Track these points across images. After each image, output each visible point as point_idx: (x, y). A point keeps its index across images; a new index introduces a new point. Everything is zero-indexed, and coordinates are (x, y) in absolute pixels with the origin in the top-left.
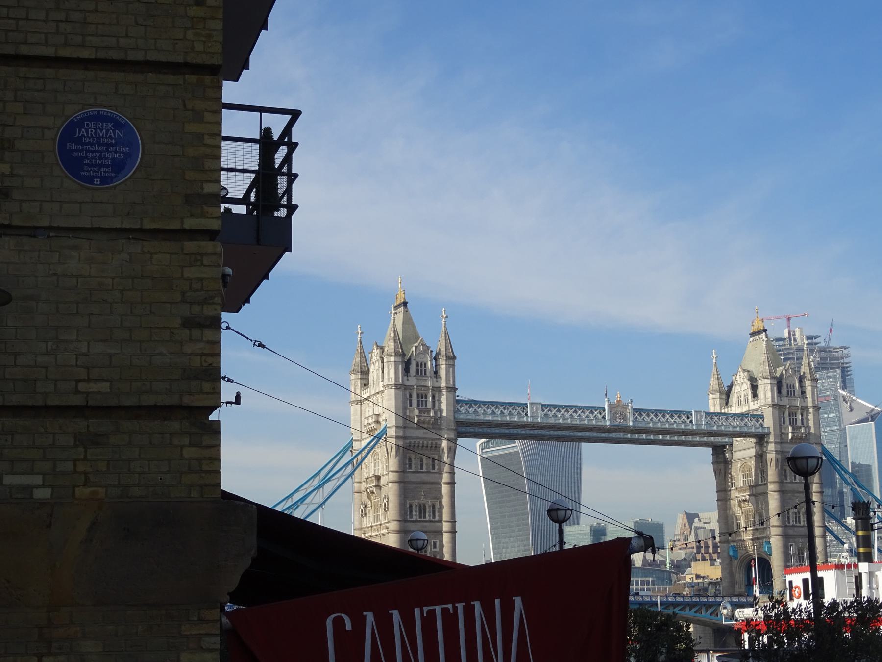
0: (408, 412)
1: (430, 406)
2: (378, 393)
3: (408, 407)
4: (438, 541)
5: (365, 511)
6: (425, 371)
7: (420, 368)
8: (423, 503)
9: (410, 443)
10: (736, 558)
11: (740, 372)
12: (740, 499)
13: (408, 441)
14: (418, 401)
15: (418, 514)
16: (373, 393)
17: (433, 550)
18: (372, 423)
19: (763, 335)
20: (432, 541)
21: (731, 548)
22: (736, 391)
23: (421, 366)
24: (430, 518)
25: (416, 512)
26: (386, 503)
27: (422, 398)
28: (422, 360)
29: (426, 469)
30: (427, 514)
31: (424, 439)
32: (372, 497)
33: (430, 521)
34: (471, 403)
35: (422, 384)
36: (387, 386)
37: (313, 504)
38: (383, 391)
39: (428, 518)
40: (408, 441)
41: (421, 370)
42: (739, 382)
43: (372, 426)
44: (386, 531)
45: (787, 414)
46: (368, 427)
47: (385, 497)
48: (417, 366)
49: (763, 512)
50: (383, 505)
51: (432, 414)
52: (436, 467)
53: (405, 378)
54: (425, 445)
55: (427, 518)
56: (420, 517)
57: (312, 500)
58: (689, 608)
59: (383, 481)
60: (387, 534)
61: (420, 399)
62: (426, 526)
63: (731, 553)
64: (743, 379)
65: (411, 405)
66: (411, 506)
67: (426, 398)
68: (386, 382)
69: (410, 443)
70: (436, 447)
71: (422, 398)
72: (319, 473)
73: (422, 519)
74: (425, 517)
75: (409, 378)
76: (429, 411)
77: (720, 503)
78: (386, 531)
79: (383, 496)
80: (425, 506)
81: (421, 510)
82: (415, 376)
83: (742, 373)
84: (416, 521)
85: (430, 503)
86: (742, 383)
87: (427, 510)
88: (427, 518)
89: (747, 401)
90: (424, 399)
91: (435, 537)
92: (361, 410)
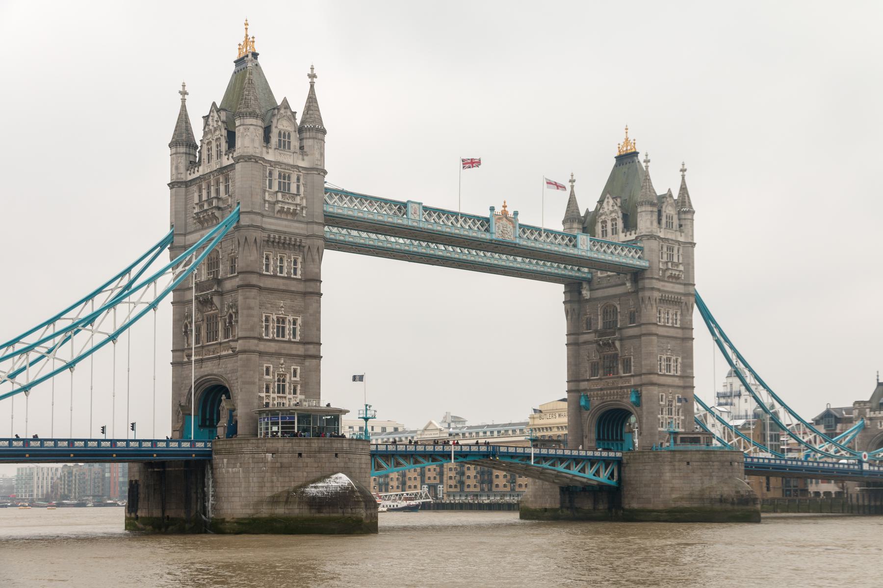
0: (267, 194)
1: (293, 189)
3: (268, 189)
4: (299, 368)
6: (289, 142)
7: (282, 139)
8: (282, 318)
9: (269, 236)
10: (587, 409)
11: (608, 198)
14: (280, 183)
15: (275, 330)
17: (293, 379)
20: (292, 367)
21: (583, 397)
23: (284, 137)
24: (290, 337)
25: (273, 329)
27: (284, 179)
33: (289, 342)
34: (342, 194)
37: (142, 303)
39: (288, 337)
41: (284, 142)
42: (606, 210)
45: (665, 249)
49: (630, 359)
52: (299, 272)
53: (264, 149)
54: (288, 242)
55: (287, 338)
56: (278, 336)
57: (141, 298)
58: (589, 464)
61: (282, 180)
62: (284, 349)
63: (583, 403)
64: (612, 206)
65: (270, 187)
66: (267, 320)
69: (269, 236)
70: (299, 246)
71: (284, 179)
73: (280, 338)
74: (283, 336)
75: (270, 151)
77: (570, 347)
80: (283, 322)
81: (279, 326)
82: (275, 149)
84: (273, 340)
85: (290, 318)
88: (287, 338)
89: (615, 231)
90: (286, 181)
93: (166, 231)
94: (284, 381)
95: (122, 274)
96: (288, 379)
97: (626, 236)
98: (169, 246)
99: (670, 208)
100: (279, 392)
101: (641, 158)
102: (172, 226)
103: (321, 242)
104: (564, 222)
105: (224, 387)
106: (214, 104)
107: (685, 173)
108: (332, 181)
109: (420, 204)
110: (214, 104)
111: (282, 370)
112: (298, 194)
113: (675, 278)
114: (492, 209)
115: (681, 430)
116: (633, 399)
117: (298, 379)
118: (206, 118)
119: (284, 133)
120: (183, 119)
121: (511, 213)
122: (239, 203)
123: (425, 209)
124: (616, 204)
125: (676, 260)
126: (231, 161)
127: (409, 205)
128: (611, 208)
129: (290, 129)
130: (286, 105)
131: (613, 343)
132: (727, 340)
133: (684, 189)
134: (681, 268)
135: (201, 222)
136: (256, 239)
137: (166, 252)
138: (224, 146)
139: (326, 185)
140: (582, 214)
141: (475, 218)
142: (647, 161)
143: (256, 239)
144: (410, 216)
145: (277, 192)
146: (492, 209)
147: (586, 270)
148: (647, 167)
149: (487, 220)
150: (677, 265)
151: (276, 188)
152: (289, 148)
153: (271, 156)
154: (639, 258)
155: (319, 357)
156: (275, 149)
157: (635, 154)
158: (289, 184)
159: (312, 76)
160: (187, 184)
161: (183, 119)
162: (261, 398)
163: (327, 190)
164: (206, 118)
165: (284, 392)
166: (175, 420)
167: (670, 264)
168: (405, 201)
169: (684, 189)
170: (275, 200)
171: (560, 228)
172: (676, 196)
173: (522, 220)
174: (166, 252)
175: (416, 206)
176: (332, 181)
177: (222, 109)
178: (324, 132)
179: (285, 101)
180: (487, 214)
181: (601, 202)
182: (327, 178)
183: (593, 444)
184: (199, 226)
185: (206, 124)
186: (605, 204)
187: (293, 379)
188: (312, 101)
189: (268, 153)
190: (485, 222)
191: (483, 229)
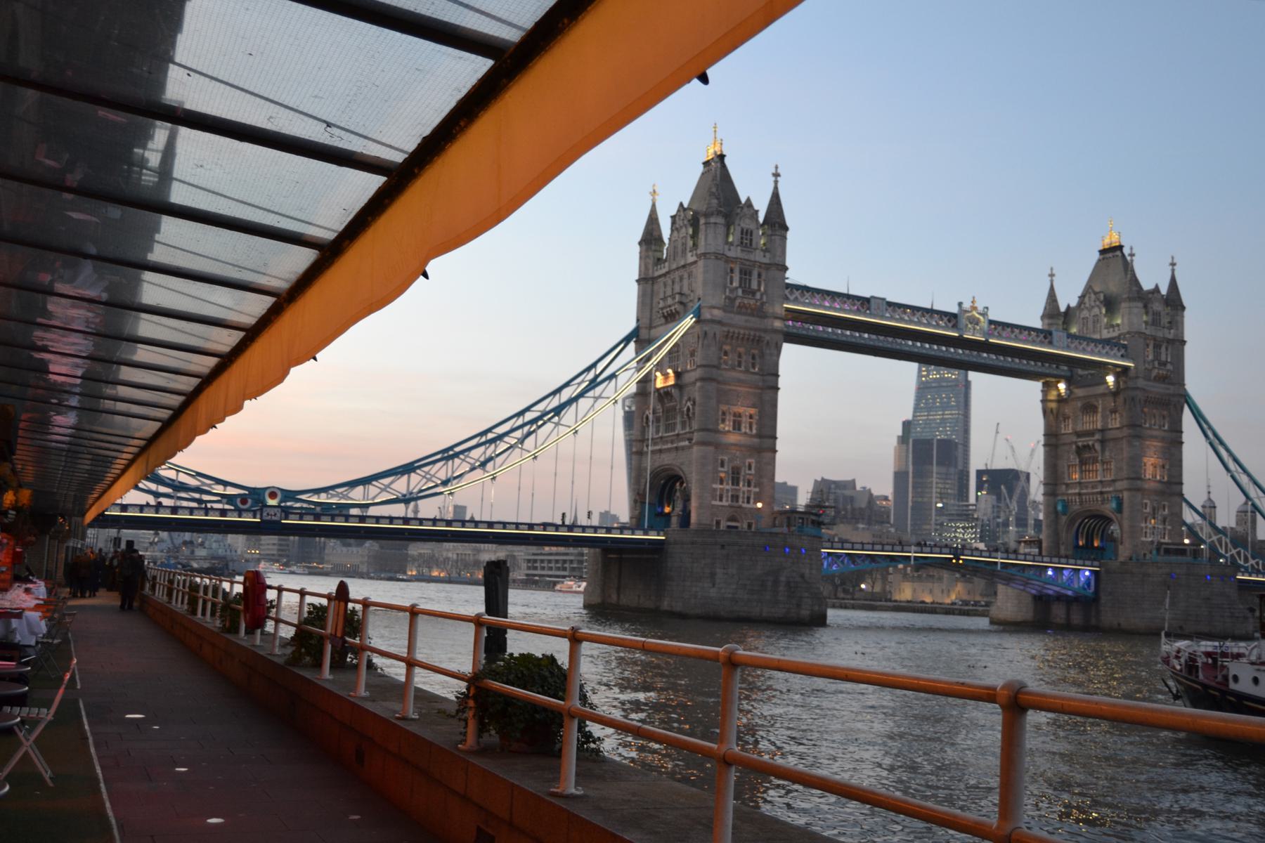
0: (727, 290)
1: (754, 285)
2: (684, 266)
3: (729, 285)
5: (693, 409)
9: (728, 332)
12: (1080, 444)
13: (726, 329)
14: (741, 279)
16: (674, 266)
17: (748, 472)
18: (674, 304)
19: (1118, 253)
22: (1082, 316)
26: (691, 407)
28: (747, 226)
29: (745, 367)
30: (743, 425)
31: (745, 328)
32: (666, 401)
34: (805, 289)
35: (746, 257)
36: (704, 254)
38: (695, 262)
40: (726, 329)
42: (1087, 305)
43: (673, 308)
44: (687, 443)
46: (665, 311)
47: (689, 399)
48: (742, 233)
50: (685, 409)
51: (758, 296)
59: (688, 378)
60: (690, 447)
65: (731, 283)
67: (750, 274)
68: (701, 250)
70: (758, 340)
72: (594, 365)
75: (732, 248)
76: (754, 293)
78: (687, 443)
79: (686, 398)
83: (1093, 296)
86: (1093, 307)
87: (744, 419)
91: (750, 457)
92: (652, 291)
93: (631, 325)
94: (738, 473)
95: (588, 369)
96: (743, 473)
97: (1109, 332)
98: (634, 339)
99: (1157, 304)
100: (733, 484)
101: (1126, 251)
102: (638, 320)
103: (781, 337)
104: (1043, 318)
105: (681, 478)
106: (681, 204)
107: (1175, 267)
108: (794, 275)
109: (884, 299)
110: (681, 204)
111: (737, 463)
112: (759, 290)
113: (1162, 379)
114: (960, 304)
115: (1167, 540)
116: (1114, 505)
117: (753, 471)
118: (673, 217)
119: (747, 231)
120: (653, 220)
121: (980, 309)
122: (699, 299)
123: (890, 304)
124: (1098, 299)
125: (1163, 358)
126: (694, 258)
127: (872, 301)
128: (1093, 304)
129: (752, 226)
130: (749, 203)
131: (1093, 445)
132: (1222, 443)
133: (1173, 284)
134: (1169, 367)
135: (665, 317)
136: (715, 334)
137: (632, 345)
138: (690, 243)
139: (787, 281)
140: (1063, 308)
141: (942, 314)
142: (1132, 255)
143: (715, 334)
144: (873, 310)
145: (737, 288)
146: (960, 304)
147: (1066, 368)
148: (1132, 261)
149: (955, 316)
150: (1165, 364)
151: (736, 284)
152: (751, 244)
153: (735, 252)
154: (1122, 356)
155: (775, 451)
156: (738, 246)
157: (1120, 248)
158: (750, 280)
159: (776, 175)
160: (654, 280)
161: (653, 220)
162: (715, 490)
163: (788, 286)
164: (673, 217)
165: (738, 485)
166: (633, 509)
167: (1156, 363)
168: (867, 295)
169: (1173, 284)
170: (735, 295)
171: (1038, 324)
172: (1164, 290)
173: (992, 316)
174: (632, 345)
175: (880, 301)
176: (794, 275)
177: (689, 209)
178: (786, 229)
179: (748, 200)
180: (955, 310)
181: (1082, 297)
182: (788, 274)
183: (1070, 553)
184: (663, 320)
185: (673, 223)
186: (1086, 300)
187: (748, 472)
188: (775, 200)
189: (730, 250)
190: (952, 319)
191: (950, 325)
